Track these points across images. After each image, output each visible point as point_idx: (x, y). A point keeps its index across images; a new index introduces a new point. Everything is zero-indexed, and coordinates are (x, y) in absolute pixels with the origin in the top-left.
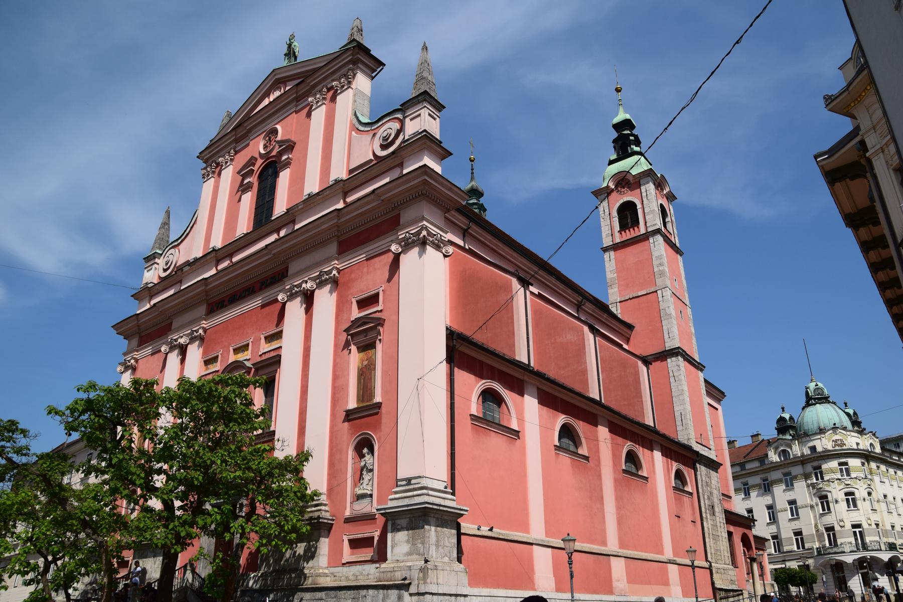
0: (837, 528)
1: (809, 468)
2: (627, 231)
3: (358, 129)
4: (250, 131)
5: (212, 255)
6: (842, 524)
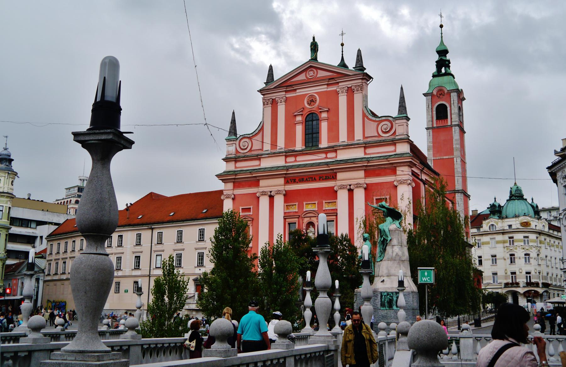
0: (518, 273)
1: (506, 237)
2: (441, 121)
3: (368, 117)
4: (295, 90)
6: (521, 271)
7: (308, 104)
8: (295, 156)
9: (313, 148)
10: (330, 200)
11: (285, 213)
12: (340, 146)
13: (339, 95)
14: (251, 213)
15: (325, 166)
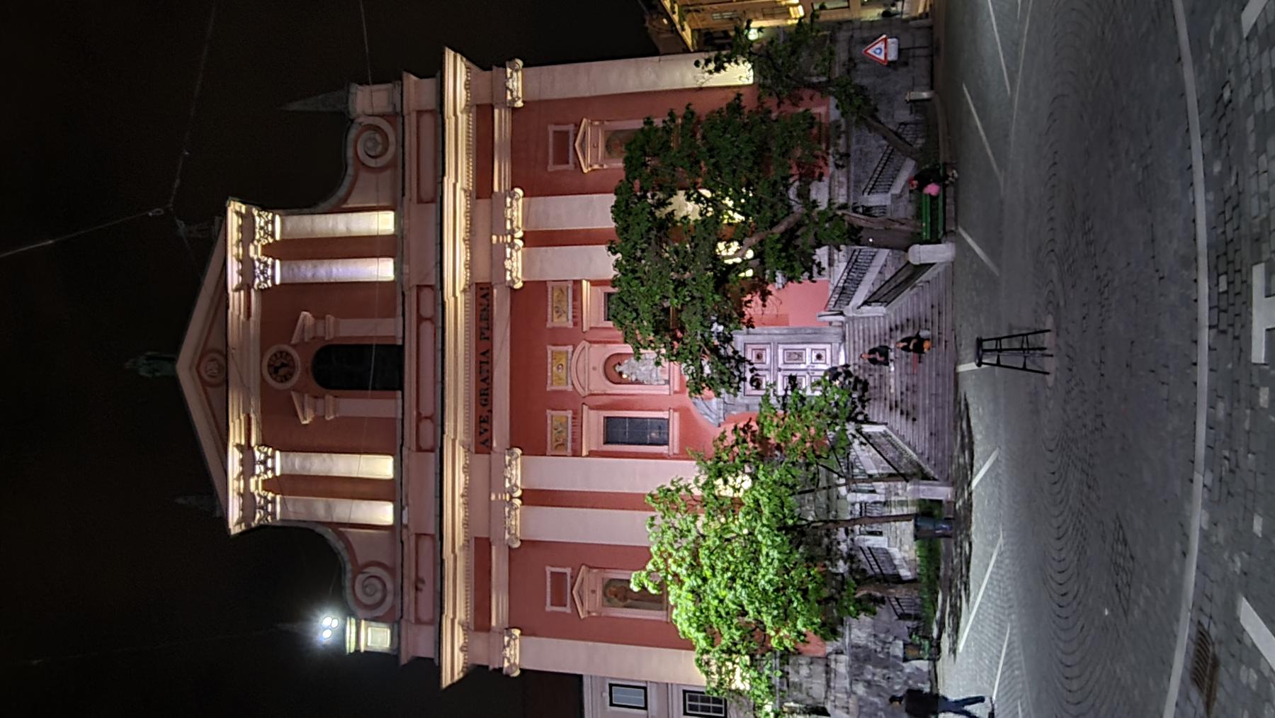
14: (568, 571)
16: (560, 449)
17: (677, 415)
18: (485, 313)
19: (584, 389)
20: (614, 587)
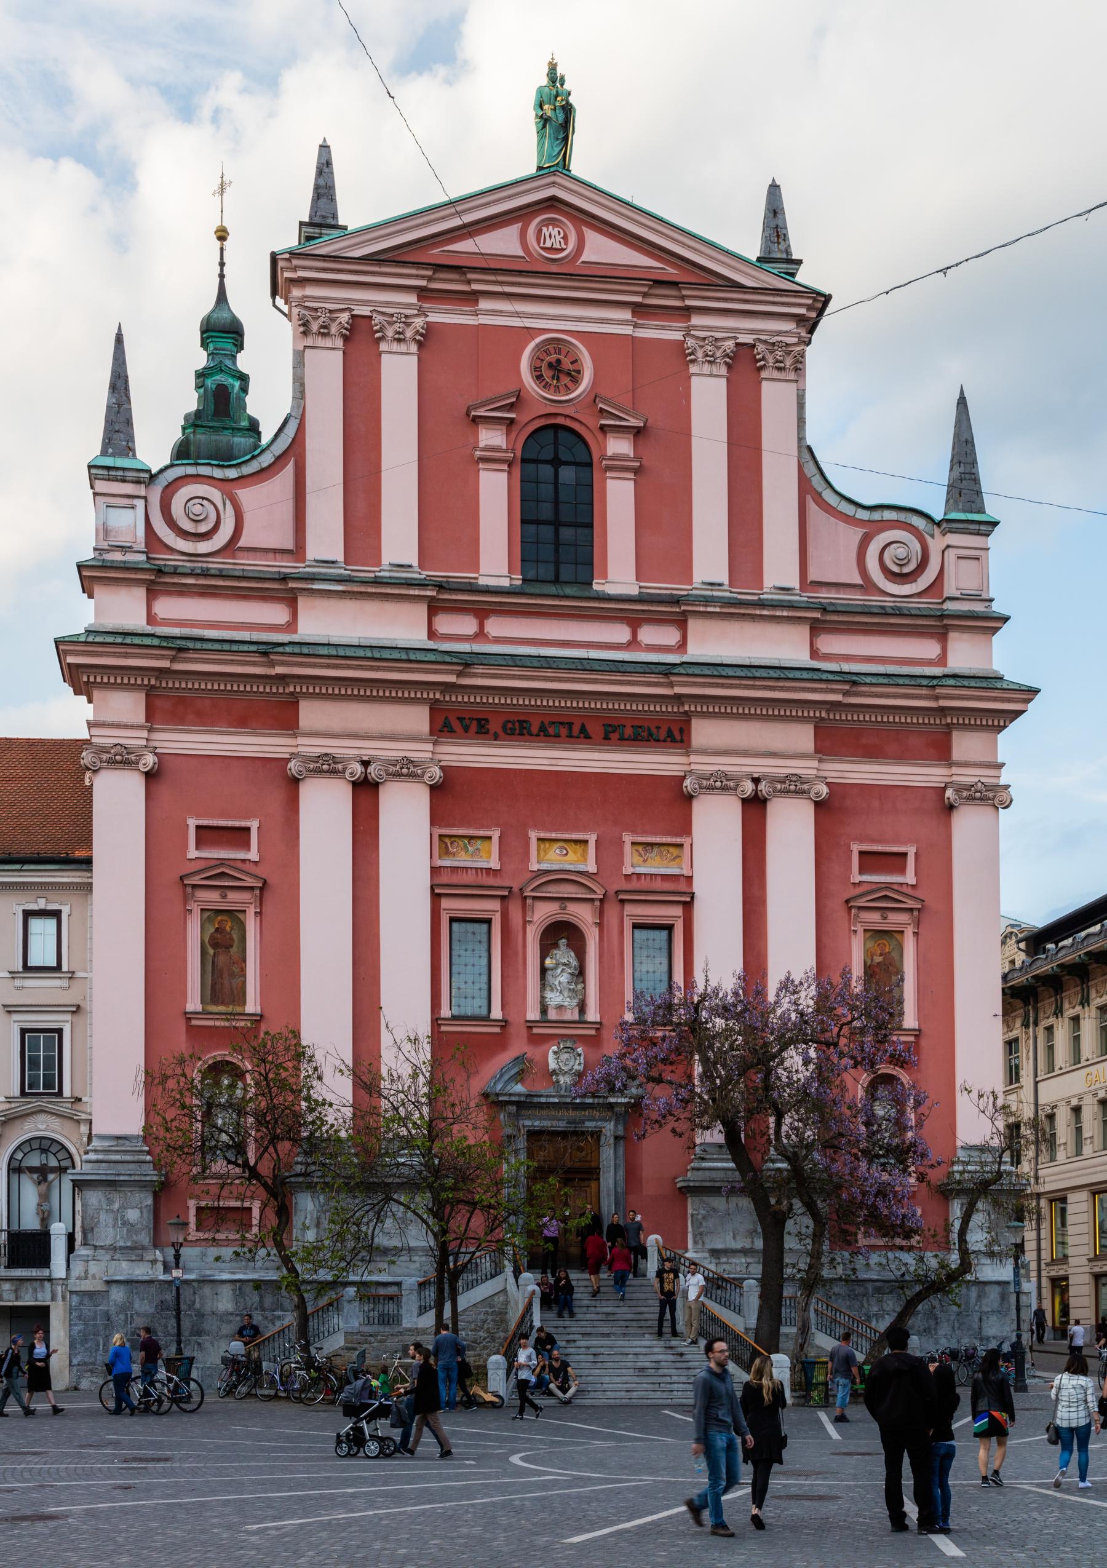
5: (429, 593)
7: (539, 378)
8: (482, 613)
9: (569, 591)
10: (655, 834)
11: (435, 871)
12: (708, 600)
13: (693, 369)
14: (253, 855)
15: (653, 679)
16: (442, 844)
17: (497, 1030)
18: (645, 734)
19: (532, 890)
20: (232, 928)
